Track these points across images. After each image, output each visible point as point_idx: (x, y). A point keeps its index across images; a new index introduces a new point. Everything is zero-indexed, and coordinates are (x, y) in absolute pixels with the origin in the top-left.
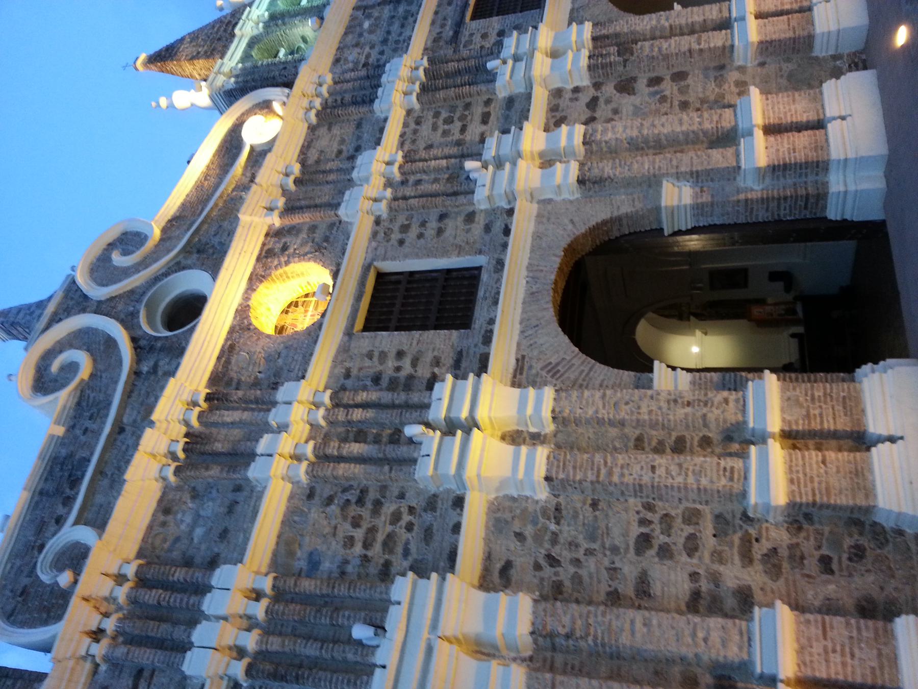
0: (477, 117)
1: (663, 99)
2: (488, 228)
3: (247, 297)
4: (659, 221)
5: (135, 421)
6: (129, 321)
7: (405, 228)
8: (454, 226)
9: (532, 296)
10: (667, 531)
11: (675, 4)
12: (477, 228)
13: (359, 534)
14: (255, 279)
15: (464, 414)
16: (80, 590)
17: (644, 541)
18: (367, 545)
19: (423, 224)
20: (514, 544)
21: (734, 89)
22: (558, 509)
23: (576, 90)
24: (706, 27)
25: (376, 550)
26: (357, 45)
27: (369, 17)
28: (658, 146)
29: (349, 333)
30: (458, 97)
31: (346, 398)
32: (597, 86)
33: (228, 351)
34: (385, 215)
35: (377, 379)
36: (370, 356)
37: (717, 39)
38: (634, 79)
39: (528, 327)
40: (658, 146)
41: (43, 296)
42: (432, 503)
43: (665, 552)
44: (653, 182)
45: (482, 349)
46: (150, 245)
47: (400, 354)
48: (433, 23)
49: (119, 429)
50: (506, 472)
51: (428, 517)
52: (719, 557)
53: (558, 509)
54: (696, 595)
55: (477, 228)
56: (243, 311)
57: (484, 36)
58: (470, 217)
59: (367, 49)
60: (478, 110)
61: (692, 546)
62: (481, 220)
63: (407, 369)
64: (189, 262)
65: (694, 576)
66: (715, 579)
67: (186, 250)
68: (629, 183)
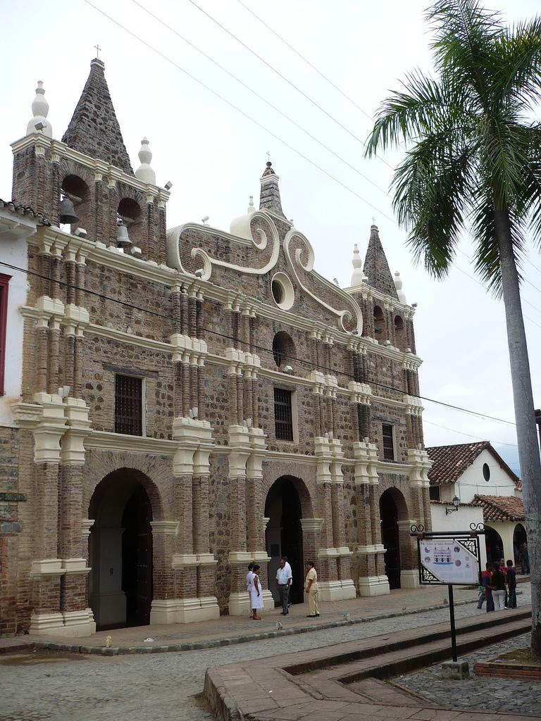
1: (348, 517)
2: (308, 444)
4: (305, 518)
5: (243, 282)
6: (276, 267)
7: (308, 404)
8: (308, 426)
12: (308, 439)
13: (215, 402)
17: (220, 516)
19: (309, 413)
22: (227, 483)
23: (354, 479)
24: (373, 534)
26: (376, 366)
27: (388, 370)
28: (334, 517)
29: (274, 384)
30: (354, 423)
32: (355, 488)
34: (313, 393)
36: (267, 396)
37: (369, 539)
38: (356, 504)
40: (334, 517)
41: (284, 211)
42: (225, 432)
43: (218, 525)
44: (322, 514)
46: (304, 267)
47: (267, 410)
48: (383, 405)
49: (240, 274)
51: (221, 431)
53: (227, 483)
55: (308, 439)
57: (376, 433)
58: (311, 435)
59: (374, 372)
60: (349, 433)
61: (220, 533)
62: (310, 440)
64: (297, 293)
67: (302, 291)
68: (322, 504)
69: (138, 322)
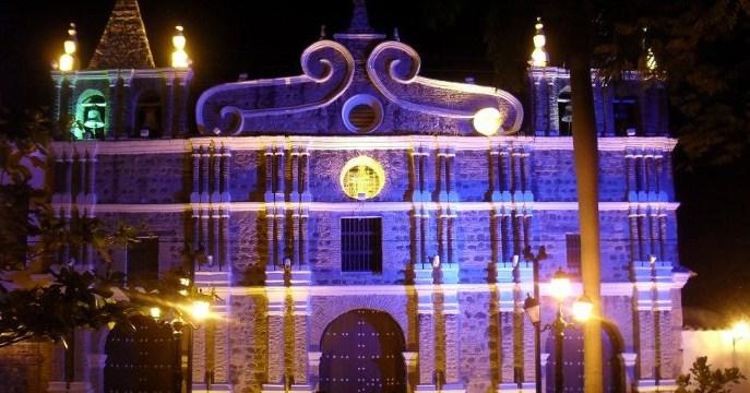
0: (480, 254)
3: (363, 153)
9: (356, 299)
10: (256, 358)
11: (548, 355)
14: (375, 154)
15: (292, 281)
16: (215, 139)
18: (243, 249)
20: (247, 306)
21: (478, 383)
25: (242, 253)
31: (305, 225)
33: (330, 154)
35: (316, 235)
39: (341, 300)
45: (330, 280)
50: (271, 301)
52: (248, 374)
54: (235, 367)
56: (356, 153)
63: (320, 248)
65: (241, 367)
66: (239, 373)
69: (153, 191)
